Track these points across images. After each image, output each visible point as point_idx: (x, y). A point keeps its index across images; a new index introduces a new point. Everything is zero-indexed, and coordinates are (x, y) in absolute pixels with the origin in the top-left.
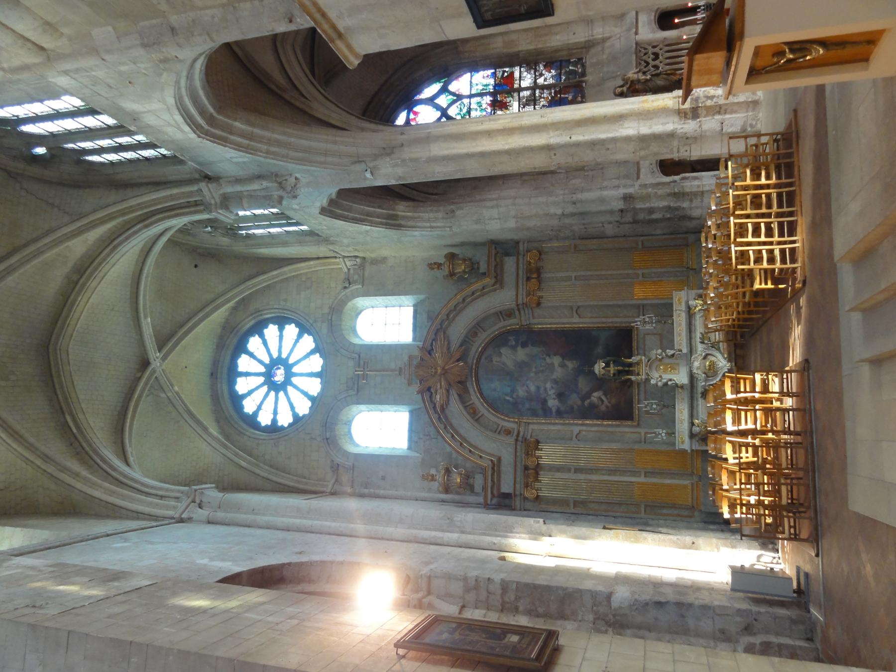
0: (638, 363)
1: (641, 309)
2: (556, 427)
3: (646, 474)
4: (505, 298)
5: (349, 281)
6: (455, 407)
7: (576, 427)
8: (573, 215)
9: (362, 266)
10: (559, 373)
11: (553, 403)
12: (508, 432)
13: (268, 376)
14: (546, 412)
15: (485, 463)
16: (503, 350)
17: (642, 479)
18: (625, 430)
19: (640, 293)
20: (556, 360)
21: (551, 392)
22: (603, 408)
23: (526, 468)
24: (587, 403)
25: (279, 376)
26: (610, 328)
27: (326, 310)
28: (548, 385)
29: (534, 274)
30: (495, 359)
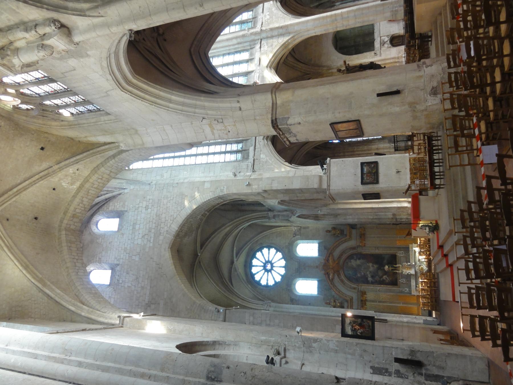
0: (399, 267)
1: (399, 248)
2: (371, 287)
3: (403, 303)
4: (352, 243)
5: (295, 235)
6: (336, 280)
7: (378, 287)
8: (376, 219)
9: (300, 229)
10: (371, 269)
11: (370, 279)
12: (354, 288)
13: (265, 267)
14: (367, 282)
15: (348, 299)
16: (352, 261)
17: (401, 305)
18: (394, 288)
19: (399, 244)
20: (371, 264)
21: (369, 275)
22: (387, 281)
23: (362, 301)
24: (381, 279)
25: (269, 267)
26: (388, 254)
27: (287, 244)
28: (368, 273)
29: (362, 236)
30: (349, 263)
